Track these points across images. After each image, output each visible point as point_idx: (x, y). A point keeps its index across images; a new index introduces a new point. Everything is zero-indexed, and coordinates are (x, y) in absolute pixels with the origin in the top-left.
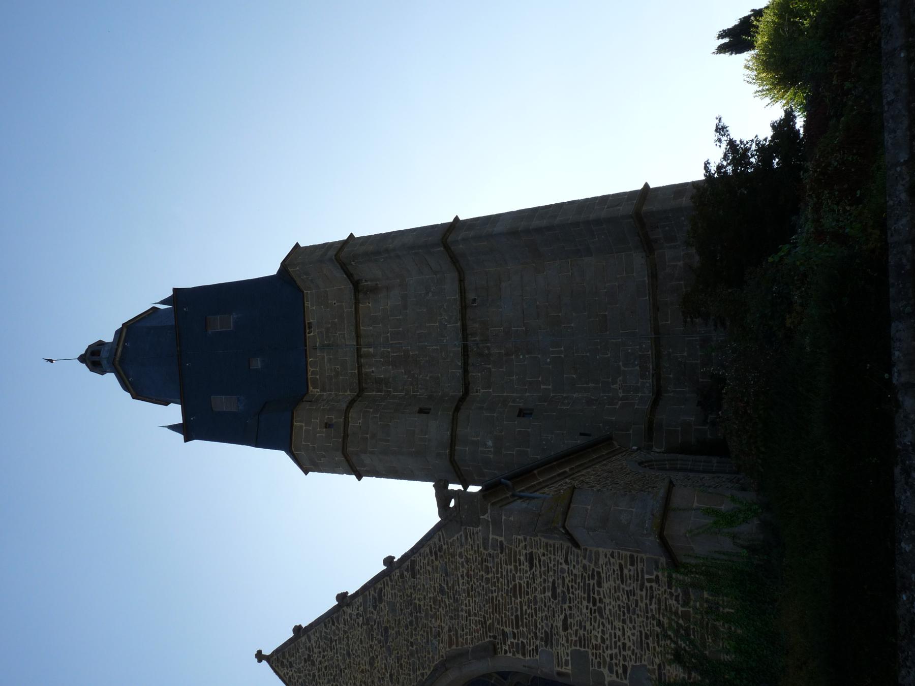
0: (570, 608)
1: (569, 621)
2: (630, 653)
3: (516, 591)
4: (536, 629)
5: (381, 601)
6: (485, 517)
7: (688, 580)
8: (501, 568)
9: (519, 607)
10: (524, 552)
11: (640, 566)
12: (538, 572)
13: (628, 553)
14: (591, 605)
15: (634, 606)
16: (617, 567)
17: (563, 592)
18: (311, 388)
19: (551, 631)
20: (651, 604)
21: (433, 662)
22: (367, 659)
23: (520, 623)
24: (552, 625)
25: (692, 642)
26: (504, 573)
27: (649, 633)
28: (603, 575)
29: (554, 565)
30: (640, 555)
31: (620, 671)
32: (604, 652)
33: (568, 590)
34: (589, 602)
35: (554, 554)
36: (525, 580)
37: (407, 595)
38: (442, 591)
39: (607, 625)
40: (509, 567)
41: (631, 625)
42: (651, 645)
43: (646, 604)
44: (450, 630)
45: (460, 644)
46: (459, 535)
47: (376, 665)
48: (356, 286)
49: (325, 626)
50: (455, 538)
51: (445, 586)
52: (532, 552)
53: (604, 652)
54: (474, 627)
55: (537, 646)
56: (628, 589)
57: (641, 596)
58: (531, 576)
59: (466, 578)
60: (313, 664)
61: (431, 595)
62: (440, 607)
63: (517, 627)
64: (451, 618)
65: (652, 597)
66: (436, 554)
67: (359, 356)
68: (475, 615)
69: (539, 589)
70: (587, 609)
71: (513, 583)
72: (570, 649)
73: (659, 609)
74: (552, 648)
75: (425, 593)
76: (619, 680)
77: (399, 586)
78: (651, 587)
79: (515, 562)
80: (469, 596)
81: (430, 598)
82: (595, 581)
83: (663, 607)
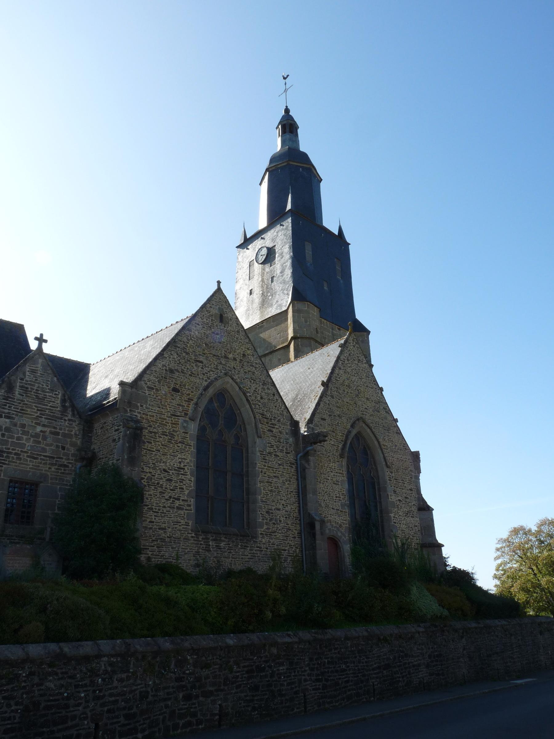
12: (409, 492)
14: (406, 512)
57: (412, 533)
79: (410, 483)
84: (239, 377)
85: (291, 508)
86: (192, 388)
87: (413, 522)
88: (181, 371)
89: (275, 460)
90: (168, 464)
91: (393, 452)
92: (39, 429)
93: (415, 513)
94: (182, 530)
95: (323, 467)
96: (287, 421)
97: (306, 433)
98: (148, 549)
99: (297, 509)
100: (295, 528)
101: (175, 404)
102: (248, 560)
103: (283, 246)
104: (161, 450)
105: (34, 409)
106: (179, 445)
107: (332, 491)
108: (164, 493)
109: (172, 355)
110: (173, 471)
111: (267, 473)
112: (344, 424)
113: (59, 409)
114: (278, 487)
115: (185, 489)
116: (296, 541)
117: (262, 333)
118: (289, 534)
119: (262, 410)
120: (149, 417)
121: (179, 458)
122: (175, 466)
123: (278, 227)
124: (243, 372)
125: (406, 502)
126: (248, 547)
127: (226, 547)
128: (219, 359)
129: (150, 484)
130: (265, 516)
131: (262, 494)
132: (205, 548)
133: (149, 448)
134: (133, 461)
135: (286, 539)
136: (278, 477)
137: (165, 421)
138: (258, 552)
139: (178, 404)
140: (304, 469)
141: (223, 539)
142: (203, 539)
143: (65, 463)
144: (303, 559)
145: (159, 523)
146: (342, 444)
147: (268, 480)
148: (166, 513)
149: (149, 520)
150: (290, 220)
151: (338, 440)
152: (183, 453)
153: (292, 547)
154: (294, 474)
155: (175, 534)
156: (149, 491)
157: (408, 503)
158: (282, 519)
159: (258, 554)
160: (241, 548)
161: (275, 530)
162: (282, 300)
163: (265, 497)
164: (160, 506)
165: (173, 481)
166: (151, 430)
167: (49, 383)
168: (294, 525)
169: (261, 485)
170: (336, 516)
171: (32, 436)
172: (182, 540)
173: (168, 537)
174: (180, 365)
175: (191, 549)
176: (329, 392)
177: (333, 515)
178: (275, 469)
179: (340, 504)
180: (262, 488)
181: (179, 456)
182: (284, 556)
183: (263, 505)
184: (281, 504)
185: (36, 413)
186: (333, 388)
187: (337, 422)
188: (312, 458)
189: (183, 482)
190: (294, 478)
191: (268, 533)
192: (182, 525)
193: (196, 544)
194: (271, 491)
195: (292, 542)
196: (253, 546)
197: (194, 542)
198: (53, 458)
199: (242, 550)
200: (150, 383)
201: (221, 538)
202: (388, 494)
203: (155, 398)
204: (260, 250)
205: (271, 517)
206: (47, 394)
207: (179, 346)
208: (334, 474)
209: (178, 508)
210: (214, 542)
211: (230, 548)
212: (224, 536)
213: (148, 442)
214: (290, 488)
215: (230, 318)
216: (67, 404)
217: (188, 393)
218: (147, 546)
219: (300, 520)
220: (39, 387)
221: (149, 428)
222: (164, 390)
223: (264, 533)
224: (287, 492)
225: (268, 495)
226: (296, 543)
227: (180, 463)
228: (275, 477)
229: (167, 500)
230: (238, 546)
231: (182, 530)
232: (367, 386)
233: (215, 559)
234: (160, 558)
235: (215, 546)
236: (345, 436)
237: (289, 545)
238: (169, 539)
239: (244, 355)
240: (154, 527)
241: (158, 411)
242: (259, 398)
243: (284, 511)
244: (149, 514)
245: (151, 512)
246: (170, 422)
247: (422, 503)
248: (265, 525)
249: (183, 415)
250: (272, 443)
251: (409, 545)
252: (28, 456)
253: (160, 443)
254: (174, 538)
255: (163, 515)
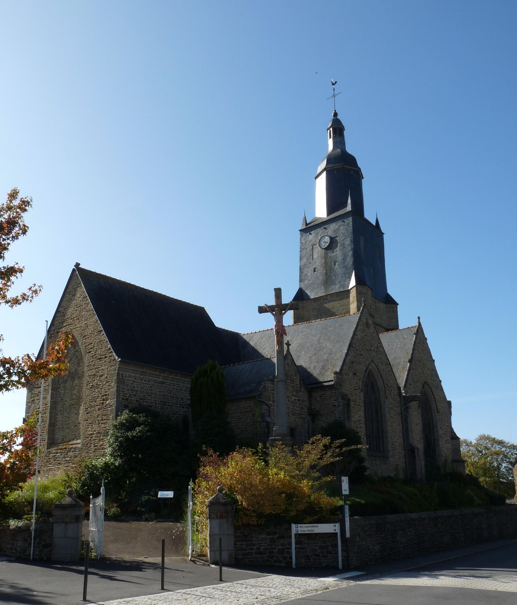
92: (294, 398)
97: (404, 394)
103: (344, 239)
106: (358, 407)
113: (299, 386)
117: (326, 303)
123: (340, 223)
125: (446, 434)
134: (349, 418)
138: (390, 467)
140: (406, 418)
143: (304, 417)
144: (407, 470)
150: (350, 219)
162: (344, 281)
185: (291, 389)
198: (299, 414)
204: (323, 238)
206: (294, 377)
216: (302, 383)
219: (405, 448)
222: (351, 374)
227: (359, 417)
228: (393, 422)
239: (377, 347)
252: (291, 414)
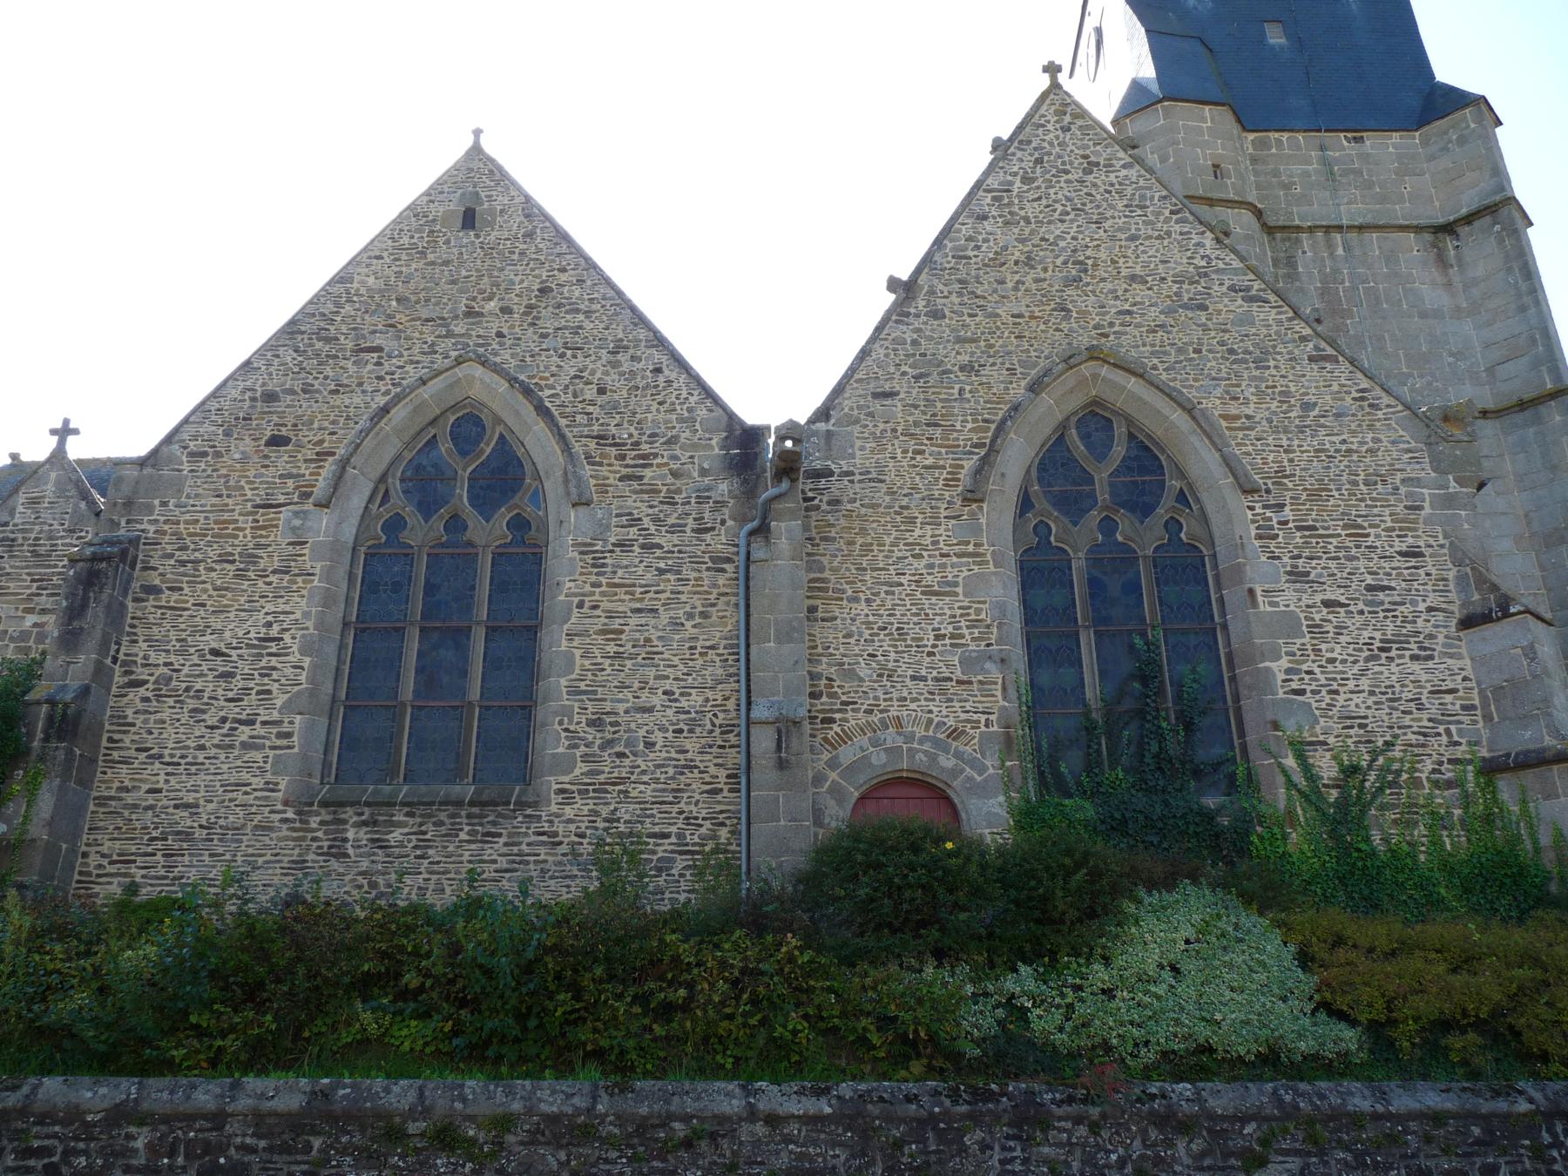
0: (1361, 612)
1: (1342, 610)
2: (1327, 700)
3: (1356, 530)
4: (1307, 558)
5: (1251, 299)
6: (1453, 484)
7: (1471, 787)
8: (1382, 506)
9: (1331, 532)
10: (1422, 544)
11: (1466, 719)
12: (1398, 564)
13: (1477, 702)
14: (1377, 644)
15: (1402, 708)
16: (1451, 686)
17: (1382, 603)
18: (1251, 136)
19: (1313, 582)
20: (1414, 733)
21: (1184, 387)
22: (1138, 270)
23: (1307, 533)
24: (1324, 583)
25: (1381, 790)
26: (1375, 511)
27: (1369, 729)
28: (1430, 664)
29: (1417, 590)
30: (1479, 718)
31: (1295, 685)
32: (1314, 661)
33: (1388, 610)
34: (1382, 641)
35: (1434, 591)
36: (1378, 544)
37: (1274, 347)
38: (1307, 407)
39: (1357, 667)
40: (1388, 519)
41: (1370, 702)
42: (1352, 732)
43: (1410, 727)
44: (1248, 417)
45: (1233, 433)
46: (1408, 438)
47: (1134, 285)
48: (1448, 229)
49: (1165, 197)
50: (1401, 433)
51: (1316, 412)
52: (1424, 556)
53: (1314, 661)
54: (1271, 458)
55: (1279, 558)
56: (1424, 700)
57: (1420, 720)
58: (1388, 554)
59: (1344, 447)
60: (1087, 172)
61: (1293, 389)
62: (1280, 401)
63: (1299, 528)
64: (1270, 421)
65: (1425, 735)
66: (1362, 399)
67: (1328, 229)
68: (1291, 461)
69: (1371, 565)
70: (1370, 638)
71: (1366, 524)
72: (1298, 610)
73: (1411, 745)
74: (1287, 581)
75: (1291, 378)
76: (1279, 683)
77: (1286, 334)
78: (1439, 734)
79: (1401, 529)
80: (1317, 451)
81: (1287, 386)
82: (1416, 652)
83: (1416, 751)
84: (513, 356)
85: (707, 700)
86: (333, 423)
87: (1424, 677)
88: (302, 390)
89: (641, 562)
90: (227, 634)
91: (1285, 432)
92: (31, 620)
93: (1441, 639)
94: (251, 806)
95: (875, 547)
96: (707, 436)
98: (135, 861)
99: (733, 700)
100: (720, 761)
101: (274, 477)
102: (493, 874)
104: (209, 603)
105: (25, 581)
106: (272, 578)
107: (915, 619)
108: (204, 712)
109: (277, 356)
110: (239, 651)
111: (605, 605)
112: (990, 388)
114: (648, 640)
115: (275, 692)
116: (719, 803)
118: (688, 781)
119: (602, 425)
120: (182, 526)
121: (267, 614)
122: (252, 635)
124: (536, 337)
126: (500, 835)
127: (409, 841)
128: (446, 326)
129: (163, 692)
130: (582, 734)
131: (577, 671)
132: (325, 850)
133: (172, 604)
135: (671, 799)
136: (655, 611)
137: (231, 526)
138: (542, 850)
139: (281, 476)
141: (400, 817)
142: (322, 823)
145: (179, 791)
146: (976, 457)
147: (605, 624)
148: (203, 764)
149: (145, 787)
151: (959, 446)
152: (282, 597)
153: (700, 821)
154: (728, 591)
155: (226, 818)
156: (156, 712)
157: (1386, 606)
158: (658, 737)
159: (538, 855)
160: (468, 842)
161: (624, 775)
163: (590, 677)
164: (187, 748)
165: (239, 677)
166: (185, 558)
167: (67, 516)
168: (715, 750)
169: (575, 644)
170: (934, 700)
171: (12, 639)
172: (248, 831)
173: (201, 826)
174: (303, 375)
175: (276, 855)
176: (921, 304)
177: (914, 700)
178: (641, 586)
179: (956, 658)
180: (578, 653)
181: (270, 607)
182: (660, 855)
183: (576, 704)
184: (660, 692)
185: (28, 587)
186: (941, 287)
187: (956, 391)
188: (783, 525)
189: (271, 675)
190: (728, 604)
191: (591, 788)
192: (254, 790)
193: (294, 839)
194: (618, 655)
195: (700, 805)
196: (523, 830)
197: (289, 833)
199: (473, 846)
200: (199, 442)
201: (393, 815)
202: (1251, 592)
203: (208, 476)
205: (610, 736)
207: (303, 328)
208: (932, 560)
209: (245, 746)
210: (365, 829)
211: (424, 845)
212: (406, 809)
213: (170, 589)
214: (701, 637)
215: (499, 208)
217: (316, 439)
218: (132, 854)
220: (41, 532)
221: (177, 553)
223: (574, 788)
224: (688, 652)
225: (603, 670)
226: (719, 808)
227: (269, 625)
229: (212, 728)
230: (457, 836)
231: (251, 806)
232: (1133, 238)
233: (360, 878)
234: (167, 885)
235: (368, 840)
236: (993, 427)
237: (682, 816)
238: (206, 831)
240: (160, 804)
241: (212, 506)
242: (590, 393)
243: (670, 712)
244: (148, 772)
245: (157, 765)
246: (250, 524)
247: (1476, 597)
248: (579, 764)
249: (296, 500)
250: (635, 512)
251: (1398, 773)
253: (208, 586)
254: (221, 827)
255: (193, 769)
